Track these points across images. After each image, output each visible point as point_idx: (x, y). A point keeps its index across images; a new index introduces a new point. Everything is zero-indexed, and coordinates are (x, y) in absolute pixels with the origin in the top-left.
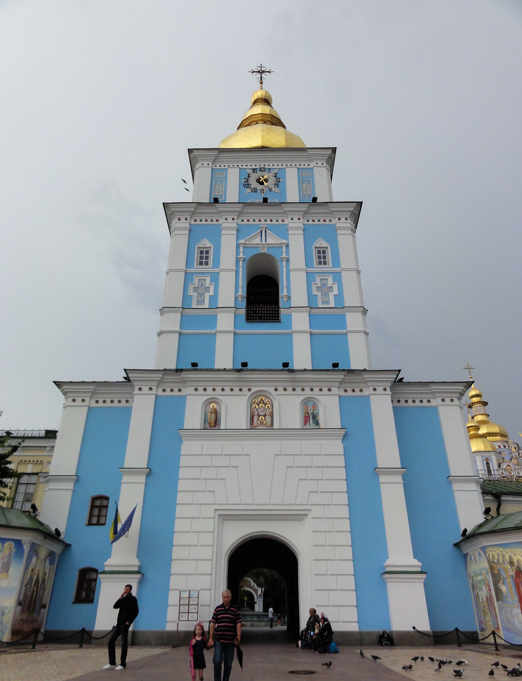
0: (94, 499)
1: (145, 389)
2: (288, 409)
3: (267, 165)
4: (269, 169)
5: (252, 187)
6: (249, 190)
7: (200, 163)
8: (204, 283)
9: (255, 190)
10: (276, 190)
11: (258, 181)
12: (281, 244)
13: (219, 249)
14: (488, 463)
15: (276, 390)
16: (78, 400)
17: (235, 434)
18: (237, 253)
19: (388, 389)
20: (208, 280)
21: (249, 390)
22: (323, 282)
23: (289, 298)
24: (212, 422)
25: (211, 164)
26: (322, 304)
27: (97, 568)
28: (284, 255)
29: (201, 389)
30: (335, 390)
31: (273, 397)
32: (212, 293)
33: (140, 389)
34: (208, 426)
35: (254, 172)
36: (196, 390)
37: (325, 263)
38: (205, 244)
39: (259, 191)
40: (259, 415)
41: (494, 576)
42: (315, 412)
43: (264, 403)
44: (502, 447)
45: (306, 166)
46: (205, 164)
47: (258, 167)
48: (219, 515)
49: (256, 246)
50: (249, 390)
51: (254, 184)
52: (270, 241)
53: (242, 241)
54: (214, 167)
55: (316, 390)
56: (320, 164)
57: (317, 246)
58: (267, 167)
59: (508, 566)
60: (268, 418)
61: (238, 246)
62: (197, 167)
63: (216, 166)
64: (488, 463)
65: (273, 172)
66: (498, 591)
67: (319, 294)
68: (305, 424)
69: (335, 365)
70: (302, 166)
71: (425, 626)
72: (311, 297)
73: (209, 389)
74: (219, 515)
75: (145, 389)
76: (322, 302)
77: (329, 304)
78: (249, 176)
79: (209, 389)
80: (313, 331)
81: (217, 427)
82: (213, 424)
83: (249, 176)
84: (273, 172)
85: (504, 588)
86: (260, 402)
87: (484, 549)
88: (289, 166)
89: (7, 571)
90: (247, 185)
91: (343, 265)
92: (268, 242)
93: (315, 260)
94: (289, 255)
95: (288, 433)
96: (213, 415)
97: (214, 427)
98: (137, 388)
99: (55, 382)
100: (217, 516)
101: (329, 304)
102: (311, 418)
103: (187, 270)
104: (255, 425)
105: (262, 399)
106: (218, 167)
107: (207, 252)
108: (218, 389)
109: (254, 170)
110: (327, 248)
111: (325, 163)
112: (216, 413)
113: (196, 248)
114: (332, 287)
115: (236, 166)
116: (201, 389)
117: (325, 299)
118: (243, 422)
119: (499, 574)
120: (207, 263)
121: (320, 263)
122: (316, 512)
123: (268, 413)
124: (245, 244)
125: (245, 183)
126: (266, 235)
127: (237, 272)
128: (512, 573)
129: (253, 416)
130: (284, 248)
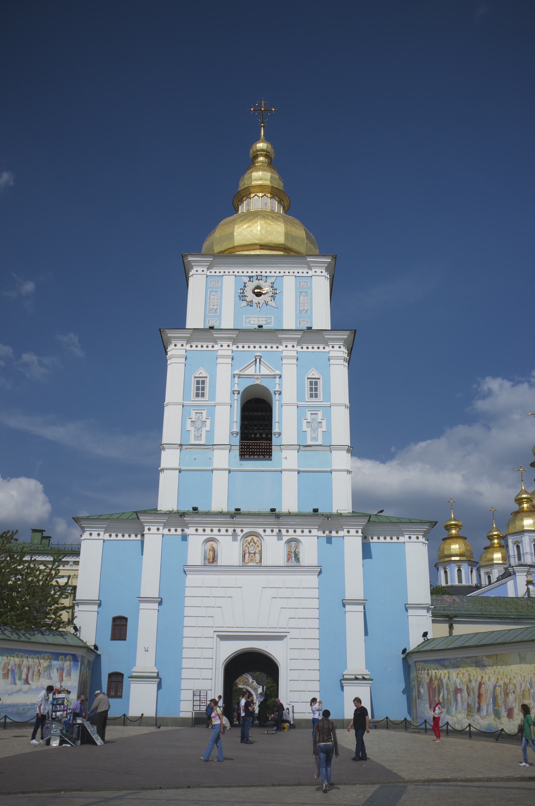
0: (115, 619)
1: (154, 529)
2: (274, 549)
3: (264, 271)
4: (266, 277)
6: (245, 303)
7: (195, 269)
8: (200, 417)
9: (250, 304)
10: (272, 303)
11: (254, 293)
12: (274, 375)
13: (215, 380)
15: (265, 531)
16: (95, 534)
17: (229, 569)
18: (232, 385)
19: (360, 531)
20: (204, 413)
21: (242, 531)
22: (313, 416)
23: (280, 434)
24: (212, 559)
25: (205, 269)
26: (311, 441)
27: (123, 673)
28: (277, 388)
29: (200, 530)
30: (315, 532)
31: (263, 538)
32: (208, 428)
33: (149, 529)
34: (207, 562)
35: (250, 281)
36: (197, 530)
37: (316, 396)
38: (201, 373)
39: (254, 305)
40: (250, 553)
41: (418, 682)
42: (297, 551)
43: (254, 542)
45: (305, 274)
46: (200, 269)
47: (254, 274)
48: (218, 636)
50: (242, 531)
51: (250, 296)
52: (265, 371)
53: (237, 372)
54: (209, 274)
55: (299, 531)
56: (319, 273)
57: (310, 376)
58: (264, 274)
59: (426, 676)
60: (257, 556)
61: (234, 376)
62: (191, 274)
63: (211, 272)
66: (419, 692)
67: (309, 430)
68: (288, 560)
69: (316, 510)
70: (300, 274)
73: (208, 530)
74: (218, 636)
75: (154, 529)
76: (311, 438)
77: (317, 441)
78: (245, 286)
79: (208, 530)
80: (300, 469)
81: (215, 564)
82: (211, 561)
83: (245, 286)
85: (422, 691)
86: (251, 541)
87: (416, 662)
88: (287, 274)
89: (70, 676)
91: (333, 401)
92: (262, 373)
94: (282, 388)
95: (274, 569)
96: (211, 552)
97: (213, 563)
98: (146, 528)
99: (73, 518)
100: (215, 637)
101: (317, 441)
102: (294, 555)
103: (184, 402)
104: (246, 562)
105: (252, 539)
106: (213, 274)
107: (203, 382)
108: (216, 530)
109: (250, 277)
110: (319, 379)
111: (324, 271)
112: (213, 550)
113: (193, 378)
114: (321, 422)
115: (231, 273)
116: (200, 530)
117: (314, 435)
118: (236, 560)
119: (421, 681)
120: (203, 395)
121: (311, 396)
122: (293, 633)
123: (257, 551)
124: (240, 375)
125: (240, 295)
126: (260, 363)
128: (428, 681)
129: (245, 554)
130: (277, 379)
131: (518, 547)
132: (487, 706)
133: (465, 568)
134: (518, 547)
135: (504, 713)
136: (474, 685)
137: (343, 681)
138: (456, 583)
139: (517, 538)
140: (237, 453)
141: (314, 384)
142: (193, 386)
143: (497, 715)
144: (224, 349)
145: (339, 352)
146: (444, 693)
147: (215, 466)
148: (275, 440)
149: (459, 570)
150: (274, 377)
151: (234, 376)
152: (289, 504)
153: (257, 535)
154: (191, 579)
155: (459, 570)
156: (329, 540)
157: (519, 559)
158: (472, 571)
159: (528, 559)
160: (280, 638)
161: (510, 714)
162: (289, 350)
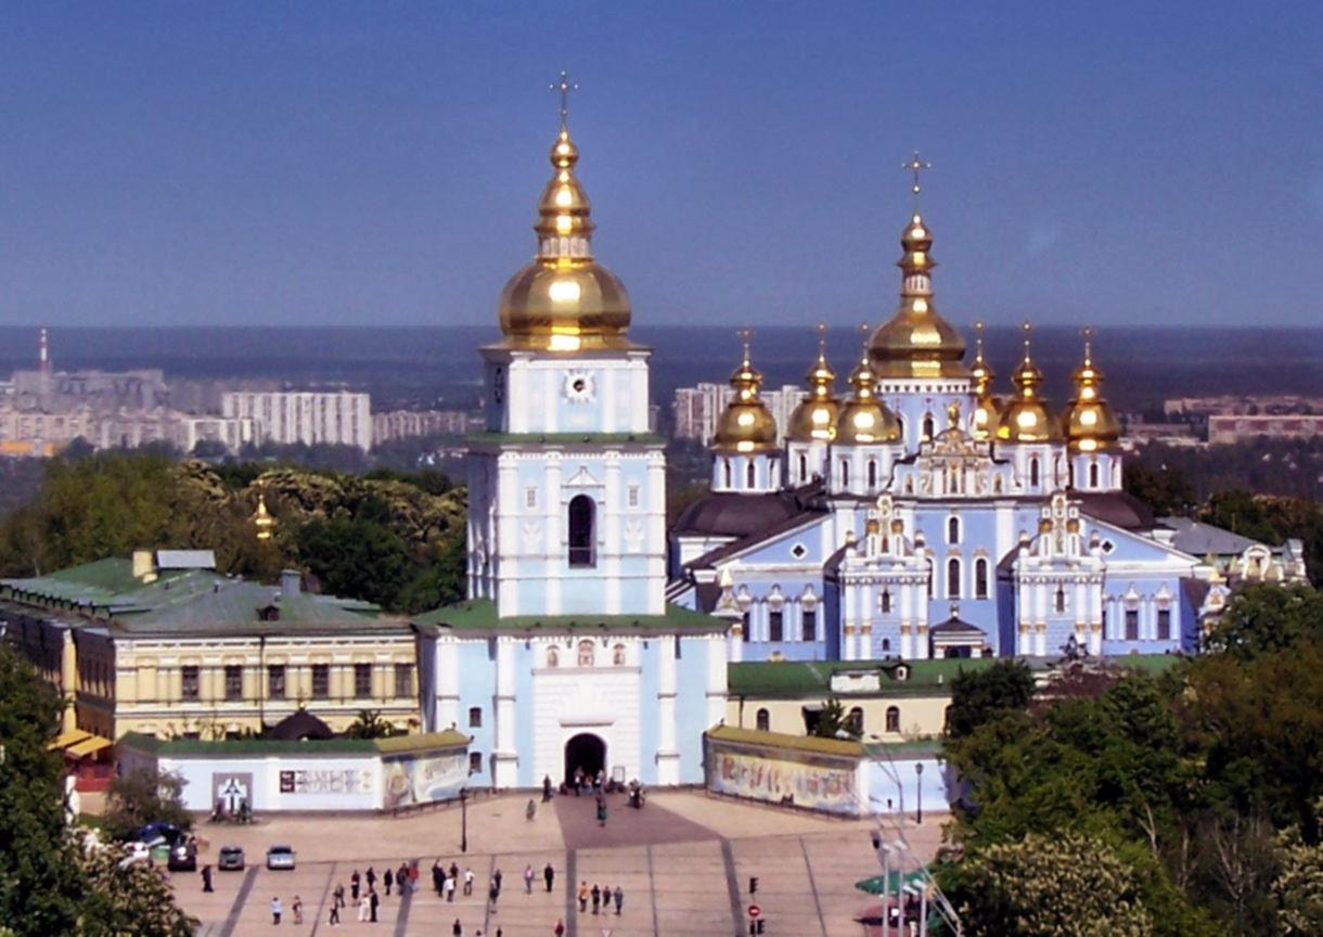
5: (570, 395)
6: (566, 401)
9: (572, 401)
10: (592, 399)
14: (872, 465)
23: (602, 544)
24: (553, 662)
28: (602, 499)
44: (934, 390)
49: (577, 487)
51: (572, 392)
52: (589, 481)
53: (565, 483)
61: (562, 487)
64: (872, 465)
65: (591, 373)
71: (675, 782)
72: (624, 542)
84: (591, 373)
90: (564, 393)
93: (628, 500)
95: (601, 670)
109: (571, 371)
112: (554, 655)
121: (631, 504)
127: (561, 517)
131: (845, 464)
132: (764, 784)
133: (761, 463)
134: (845, 464)
135: (774, 788)
136: (757, 768)
137: (658, 757)
138: (745, 489)
139: (845, 450)
140: (566, 561)
141: (633, 492)
142: (526, 496)
143: (770, 789)
144: (553, 458)
145: (657, 459)
146: (733, 771)
147: (549, 575)
148: (600, 550)
149: (751, 467)
150: (599, 487)
151: (562, 487)
152: (613, 608)
153: (591, 643)
154: (540, 680)
155: (751, 467)
156: (646, 645)
157: (846, 483)
158: (772, 466)
159: (859, 487)
160: (609, 724)
161: (778, 789)
162: (612, 458)
